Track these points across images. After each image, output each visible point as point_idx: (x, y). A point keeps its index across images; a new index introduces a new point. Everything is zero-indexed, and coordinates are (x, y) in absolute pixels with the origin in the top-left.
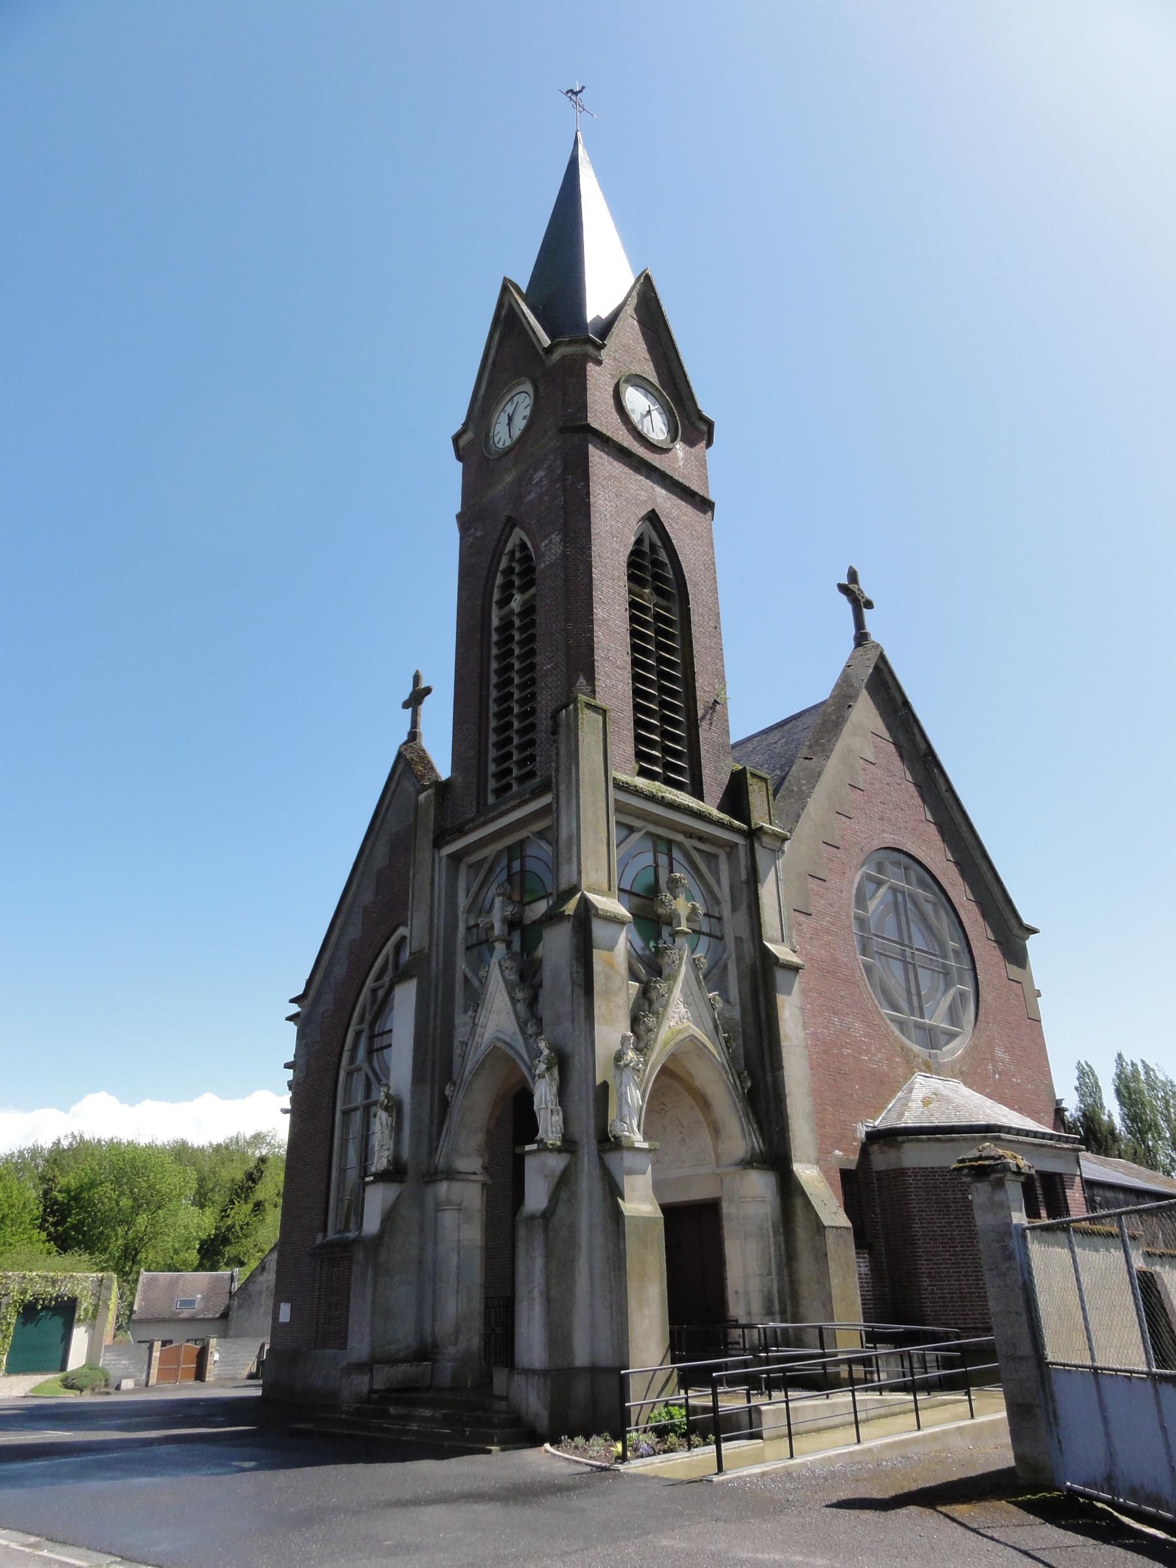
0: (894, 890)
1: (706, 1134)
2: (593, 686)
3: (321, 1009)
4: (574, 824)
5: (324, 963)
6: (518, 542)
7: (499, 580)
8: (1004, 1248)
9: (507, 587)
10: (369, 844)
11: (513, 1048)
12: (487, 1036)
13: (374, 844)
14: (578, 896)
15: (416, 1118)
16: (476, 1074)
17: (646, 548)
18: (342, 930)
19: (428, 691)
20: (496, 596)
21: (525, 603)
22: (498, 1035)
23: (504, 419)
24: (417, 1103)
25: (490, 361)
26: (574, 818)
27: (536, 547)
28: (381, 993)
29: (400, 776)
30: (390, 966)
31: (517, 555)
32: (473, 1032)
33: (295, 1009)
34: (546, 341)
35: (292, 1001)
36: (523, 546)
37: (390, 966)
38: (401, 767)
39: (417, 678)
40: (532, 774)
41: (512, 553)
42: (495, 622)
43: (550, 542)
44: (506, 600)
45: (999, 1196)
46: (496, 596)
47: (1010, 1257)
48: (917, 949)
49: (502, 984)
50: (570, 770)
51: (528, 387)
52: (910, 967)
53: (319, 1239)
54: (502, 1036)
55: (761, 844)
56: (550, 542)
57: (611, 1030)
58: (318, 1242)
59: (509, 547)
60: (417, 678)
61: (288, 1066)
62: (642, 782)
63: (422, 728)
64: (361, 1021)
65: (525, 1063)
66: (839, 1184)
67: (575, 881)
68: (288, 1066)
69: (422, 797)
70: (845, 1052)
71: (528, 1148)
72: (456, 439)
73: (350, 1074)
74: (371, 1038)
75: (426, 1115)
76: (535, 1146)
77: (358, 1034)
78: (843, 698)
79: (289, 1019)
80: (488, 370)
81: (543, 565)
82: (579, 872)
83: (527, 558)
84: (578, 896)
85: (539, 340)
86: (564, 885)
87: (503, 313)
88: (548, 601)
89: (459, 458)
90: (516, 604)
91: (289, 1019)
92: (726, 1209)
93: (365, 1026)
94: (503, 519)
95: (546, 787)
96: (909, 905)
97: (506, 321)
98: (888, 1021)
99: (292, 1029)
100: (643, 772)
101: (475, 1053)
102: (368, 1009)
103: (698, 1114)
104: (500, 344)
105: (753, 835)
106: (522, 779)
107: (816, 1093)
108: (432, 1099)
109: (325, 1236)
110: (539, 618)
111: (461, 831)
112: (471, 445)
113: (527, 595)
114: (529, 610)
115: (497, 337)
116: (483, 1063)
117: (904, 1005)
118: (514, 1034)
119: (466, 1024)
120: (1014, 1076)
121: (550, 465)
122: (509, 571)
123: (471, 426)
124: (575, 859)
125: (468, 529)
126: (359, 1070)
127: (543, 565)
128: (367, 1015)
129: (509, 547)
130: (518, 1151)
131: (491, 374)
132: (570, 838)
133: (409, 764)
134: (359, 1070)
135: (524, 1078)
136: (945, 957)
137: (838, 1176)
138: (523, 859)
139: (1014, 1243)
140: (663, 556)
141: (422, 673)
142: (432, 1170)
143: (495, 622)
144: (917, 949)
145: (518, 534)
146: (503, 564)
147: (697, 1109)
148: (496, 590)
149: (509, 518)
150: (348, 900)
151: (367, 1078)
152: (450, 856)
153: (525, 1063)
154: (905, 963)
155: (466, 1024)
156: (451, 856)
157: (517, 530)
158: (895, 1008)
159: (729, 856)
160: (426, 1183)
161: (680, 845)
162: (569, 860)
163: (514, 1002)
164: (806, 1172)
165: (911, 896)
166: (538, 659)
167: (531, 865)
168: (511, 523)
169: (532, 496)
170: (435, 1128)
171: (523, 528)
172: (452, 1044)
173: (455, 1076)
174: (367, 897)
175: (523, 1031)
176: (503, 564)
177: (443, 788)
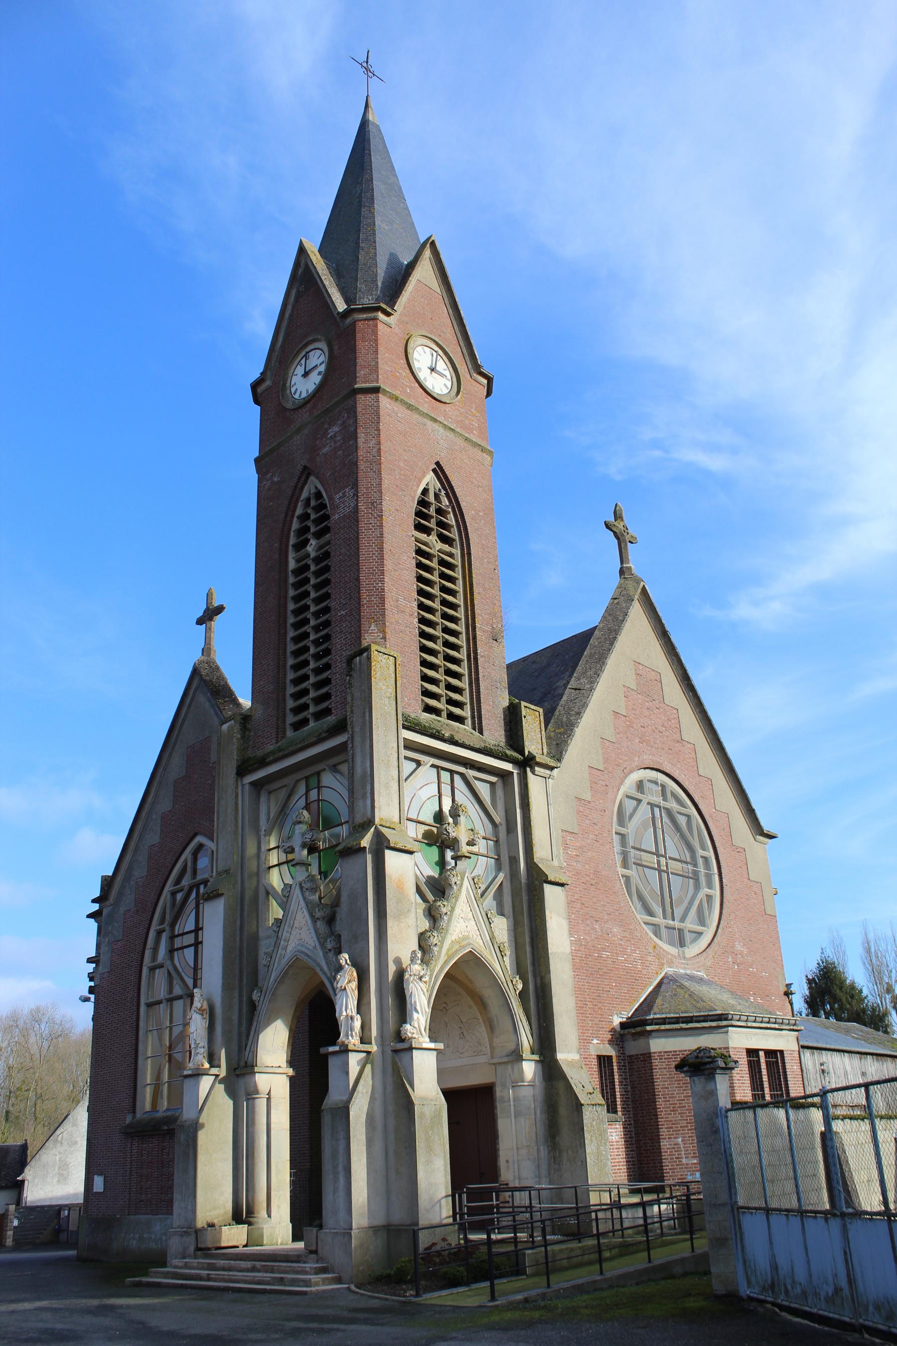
0: (652, 805)
1: (482, 1031)
2: (384, 632)
3: (122, 910)
4: (368, 764)
5: (124, 866)
6: (313, 490)
7: (295, 525)
8: (713, 1125)
9: (304, 530)
10: (166, 755)
11: (314, 961)
12: (290, 948)
13: (170, 755)
14: (372, 829)
15: (227, 1020)
16: (281, 981)
17: (431, 498)
18: (141, 838)
19: (220, 609)
20: (292, 540)
21: (320, 548)
22: (300, 948)
23: (300, 370)
24: (227, 1006)
25: (287, 315)
26: (368, 758)
27: (331, 499)
28: (179, 896)
29: (196, 690)
30: (189, 870)
31: (313, 503)
32: (277, 945)
33: (96, 907)
34: (341, 306)
35: (94, 901)
36: (318, 495)
37: (189, 870)
38: (195, 683)
39: (209, 596)
40: (327, 712)
41: (308, 500)
42: (292, 565)
43: (344, 496)
44: (301, 545)
45: (710, 1086)
46: (292, 540)
47: (716, 1131)
48: (670, 858)
49: (302, 903)
50: (364, 713)
51: (323, 345)
52: (665, 875)
53: (129, 1119)
54: (304, 949)
55: (533, 772)
56: (344, 496)
57: (402, 942)
58: (127, 1122)
59: (304, 495)
60: (209, 596)
61: (89, 960)
62: (426, 718)
63: (215, 644)
64: (162, 922)
65: (325, 973)
66: (595, 1068)
67: (369, 817)
68: (89, 960)
69: (225, 727)
70: (605, 954)
71: (331, 1049)
72: (255, 386)
73: (152, 969)
74: (172, 937)
75: (235, 1017)
76: (337, 1048)
77: (159, 933)
78: (615, 618)
79: (89, 916)
80: (285, 324)
81: (337, 517)
82: (373, 807)
83: (322, 506)
84: (372, 829)
85: (333, 306)
86: (359, 819)
87: (300, 271)
88: (343, 550)
89: (256, 401)
90: (311, 548)
91: (89, 916)
92: (499, 1092)
93: (166, 925)
94: (300, 468)
95: (341, 727)
96: (666, 819)
97: (303, 277)
98: (643, 925)
99: (93, 925)
100: (428, 709)
101: (279, 964)
102: (168, 911)
103: (475, 1010)
104: (297, 300)
105: (527, 763)
106: (318, 716)
107: (578, 991)
108: (241, 1001)
109: (134, 1117)
110: (333, 562)
111: (263, 763)
112: (267, 391)
113: (323, 540)
114: (324, 556)
115: (294, 292)
116: (286, 973)
117: (658, 910)
118: (315, 947)
119: (268, 937)
120: (751, 966)
121: (344, 422)
122: (305, 517)
123: (269, 373)
124: (369, 795)
125: (266, 473)
126: (161, 966)
127: (337, 517)
128: (168, 917)
129: (304, 495)
130: (323, 1050)
131: (288, 327)
132: (364, 776)
133: (205, 685)
134: (161, 966)
135: (322, 983)
136: (695, 865)
137: (595, 1062)
138: (319, 788)
139: (719, 1122)
140: (451, 520)
141: (214, 590)
142: (242, 1064)
143: (292, 565)
144: (670, 858)
145: (313, 485)
146: (299, 511)
147: (475, 1008)
148: (292, 534)
149: (305, 467)
150: (147, 807)
151: (169, 973)
152: (252, 784)
153: (325, 973)
154: (660, 871)
155: (268, 937)
156: (253, 784)
157: (312, 478)
158: (651, 913)
159: (505, 784)
160: (238, 1076)
161: (462, 775)
162: (364, 796)
163: (314, 920)
164: (567, 1054)
165: (669, 812)
166: (332, 603)
167: (326, 794)
168: (306, 472)
169: (325, 450)
170: (244, 1028)
171: (317, 478)
172: (257, 956)
173: (260, 984)
174: (165, 805)
175: (322, 945)
176: (299, 511)
177: (246, 719)
